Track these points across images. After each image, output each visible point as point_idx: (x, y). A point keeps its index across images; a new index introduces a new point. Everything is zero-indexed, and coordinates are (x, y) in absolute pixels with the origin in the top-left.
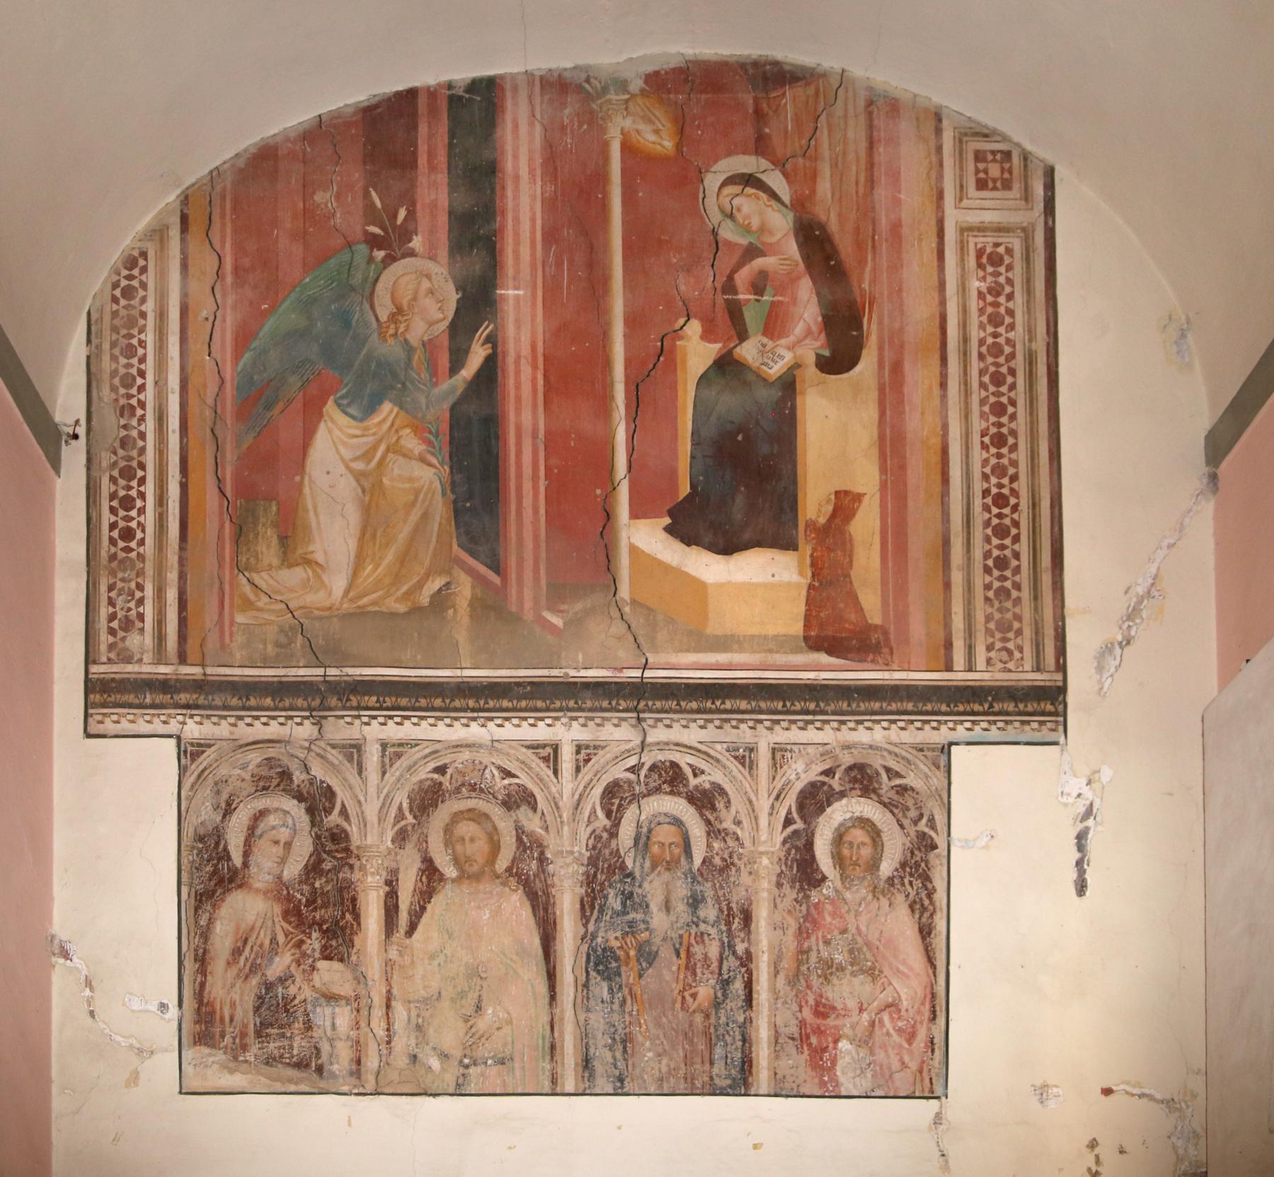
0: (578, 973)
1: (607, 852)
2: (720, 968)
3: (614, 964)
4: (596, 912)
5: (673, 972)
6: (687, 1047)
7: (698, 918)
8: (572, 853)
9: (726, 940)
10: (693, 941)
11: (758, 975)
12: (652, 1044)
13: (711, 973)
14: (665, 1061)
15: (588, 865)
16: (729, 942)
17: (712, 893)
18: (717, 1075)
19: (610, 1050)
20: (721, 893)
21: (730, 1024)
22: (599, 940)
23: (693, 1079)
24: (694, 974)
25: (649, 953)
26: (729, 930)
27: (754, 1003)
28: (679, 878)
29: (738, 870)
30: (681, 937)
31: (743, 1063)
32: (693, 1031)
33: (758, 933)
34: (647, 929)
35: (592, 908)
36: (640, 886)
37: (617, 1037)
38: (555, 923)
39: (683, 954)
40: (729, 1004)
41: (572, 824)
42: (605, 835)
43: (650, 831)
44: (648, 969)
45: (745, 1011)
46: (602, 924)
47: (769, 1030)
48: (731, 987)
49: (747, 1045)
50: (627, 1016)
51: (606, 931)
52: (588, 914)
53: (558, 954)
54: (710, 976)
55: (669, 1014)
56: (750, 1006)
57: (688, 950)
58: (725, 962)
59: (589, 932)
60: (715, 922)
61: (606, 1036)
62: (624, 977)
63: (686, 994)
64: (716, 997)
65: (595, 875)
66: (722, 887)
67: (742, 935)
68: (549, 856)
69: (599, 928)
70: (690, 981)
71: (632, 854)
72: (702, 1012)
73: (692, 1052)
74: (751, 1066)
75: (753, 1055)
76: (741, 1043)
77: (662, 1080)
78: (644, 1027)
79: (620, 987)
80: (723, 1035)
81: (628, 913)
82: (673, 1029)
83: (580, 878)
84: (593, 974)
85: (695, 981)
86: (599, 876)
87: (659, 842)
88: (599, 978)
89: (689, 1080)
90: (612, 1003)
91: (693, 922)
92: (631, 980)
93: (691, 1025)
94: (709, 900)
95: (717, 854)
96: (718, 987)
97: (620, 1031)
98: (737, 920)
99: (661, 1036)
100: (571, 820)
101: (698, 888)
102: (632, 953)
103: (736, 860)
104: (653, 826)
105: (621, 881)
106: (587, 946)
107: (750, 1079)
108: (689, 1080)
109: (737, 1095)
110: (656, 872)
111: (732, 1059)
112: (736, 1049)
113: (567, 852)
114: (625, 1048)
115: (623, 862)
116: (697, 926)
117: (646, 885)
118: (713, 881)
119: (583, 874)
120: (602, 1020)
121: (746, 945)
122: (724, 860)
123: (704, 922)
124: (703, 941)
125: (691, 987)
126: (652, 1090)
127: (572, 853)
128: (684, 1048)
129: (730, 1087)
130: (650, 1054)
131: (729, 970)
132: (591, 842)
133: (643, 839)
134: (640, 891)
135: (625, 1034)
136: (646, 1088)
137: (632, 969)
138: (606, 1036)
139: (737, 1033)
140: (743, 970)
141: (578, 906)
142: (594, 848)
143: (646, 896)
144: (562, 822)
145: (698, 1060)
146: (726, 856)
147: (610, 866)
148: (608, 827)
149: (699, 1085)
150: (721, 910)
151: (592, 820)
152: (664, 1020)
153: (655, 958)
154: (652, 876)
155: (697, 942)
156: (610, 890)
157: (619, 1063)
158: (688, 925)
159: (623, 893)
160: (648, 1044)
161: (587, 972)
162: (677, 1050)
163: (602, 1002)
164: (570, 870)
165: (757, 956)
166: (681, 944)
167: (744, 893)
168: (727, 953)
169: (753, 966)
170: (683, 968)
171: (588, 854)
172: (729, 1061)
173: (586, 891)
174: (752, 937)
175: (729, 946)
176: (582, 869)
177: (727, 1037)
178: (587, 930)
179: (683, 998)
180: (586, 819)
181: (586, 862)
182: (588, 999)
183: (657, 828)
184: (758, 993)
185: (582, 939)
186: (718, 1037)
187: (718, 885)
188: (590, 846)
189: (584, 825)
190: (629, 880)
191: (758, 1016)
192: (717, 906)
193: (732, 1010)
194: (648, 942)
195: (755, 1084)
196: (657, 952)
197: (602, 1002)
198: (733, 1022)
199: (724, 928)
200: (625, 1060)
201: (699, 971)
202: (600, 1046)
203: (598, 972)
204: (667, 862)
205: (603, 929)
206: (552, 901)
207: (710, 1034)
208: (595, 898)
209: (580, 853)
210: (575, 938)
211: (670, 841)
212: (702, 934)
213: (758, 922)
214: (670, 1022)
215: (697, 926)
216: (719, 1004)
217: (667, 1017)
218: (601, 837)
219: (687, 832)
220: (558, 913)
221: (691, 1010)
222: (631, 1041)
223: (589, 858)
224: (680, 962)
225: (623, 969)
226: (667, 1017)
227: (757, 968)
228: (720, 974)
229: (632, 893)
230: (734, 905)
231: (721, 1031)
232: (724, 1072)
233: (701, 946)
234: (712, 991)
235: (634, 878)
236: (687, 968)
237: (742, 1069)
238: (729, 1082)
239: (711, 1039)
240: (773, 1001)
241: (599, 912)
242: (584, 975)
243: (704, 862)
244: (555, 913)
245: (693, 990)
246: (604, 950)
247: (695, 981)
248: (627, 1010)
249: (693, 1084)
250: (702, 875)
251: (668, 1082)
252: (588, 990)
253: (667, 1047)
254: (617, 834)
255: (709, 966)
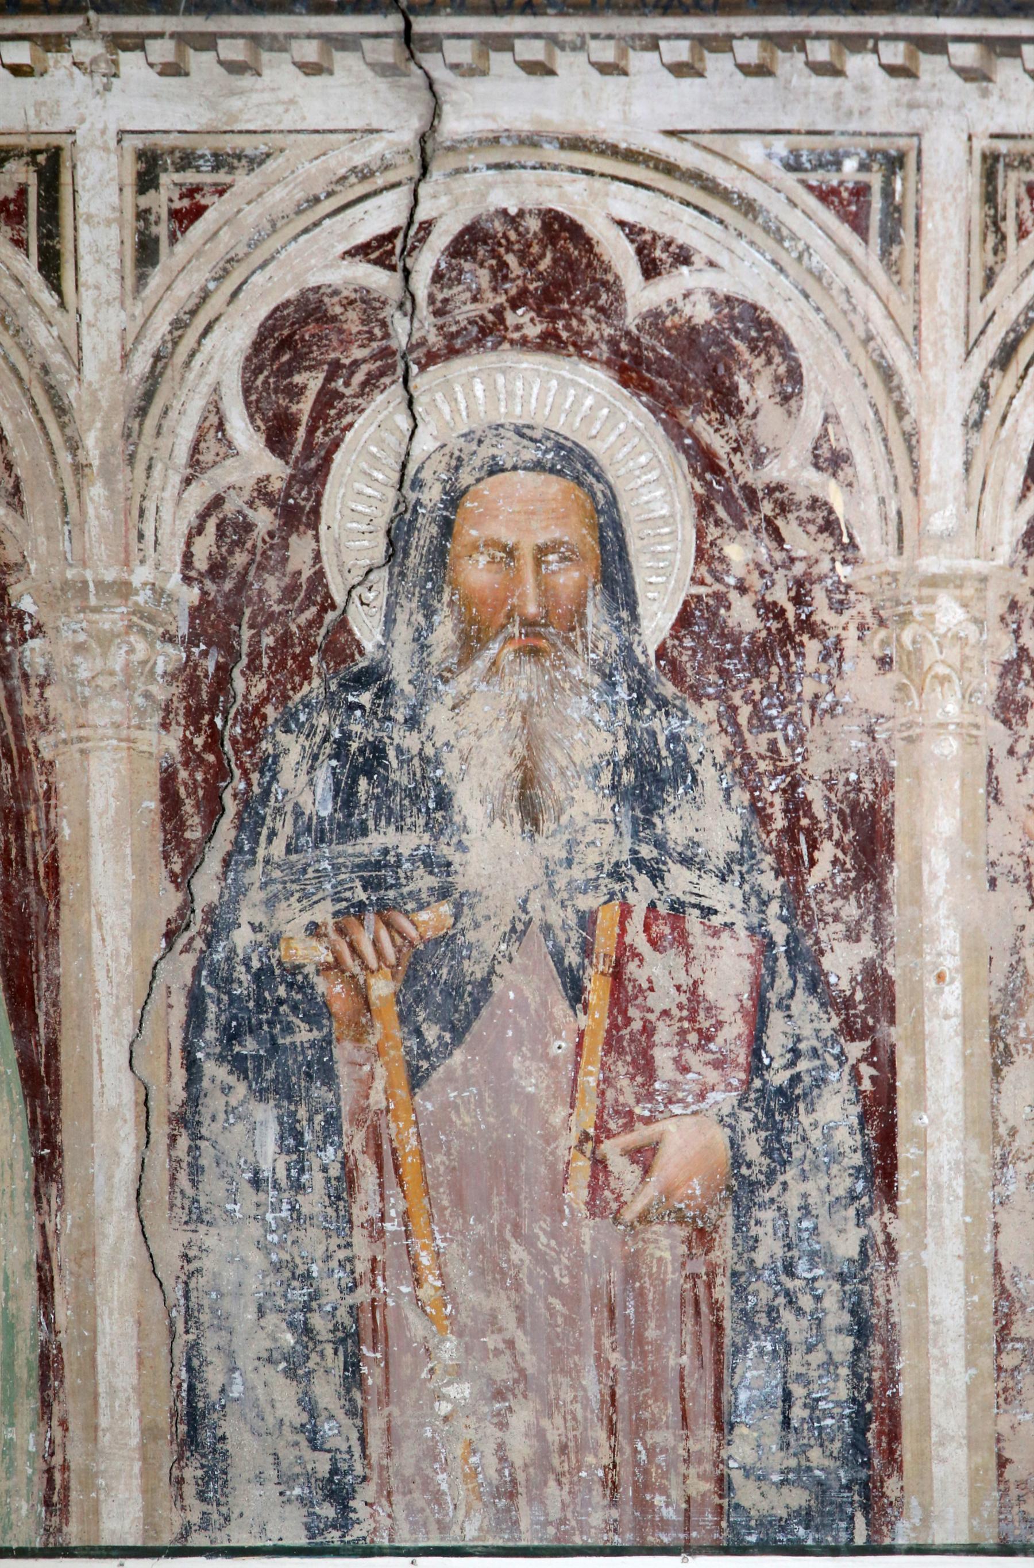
0: (152, 1069)
1: (272, 585)
2: (756, 1044)
3: (304, 1034)
4: (226, 829)
5: (553, 1064)
6: (615, 1358)
7: (660, 844)
8: (124, 589)
9: (779, 932)
10: (635, 936)
11: (920, 1067)
12: (468, 1350)
13: (718, 1064)
14: (522, 1417)
15: (192, 640)
16: (793, 939)
17: (721, 743)
18: (747, 1472)
19: (291, 1373)
20: (757, 743)
21: (802, 1267)
22: (242, 937)
23: (643, 1487)
24: (645, 1067)
25: (453, 990)
26: (795, 893)
27: (904, 1180)
28: (580, 687)
29: (833, 652)
30: (587, 921)
31: (860, 1422)
32: (641, 1294)
33: (917, 900)
34: (444, 893)
35: (213, 810)
36: (413, 722)
37: (319, 1323)
38: (53, 870)
39: (597, 989)
40: (796, 1188)
41: (122, 477)
42: (264, 519)
43: (454, 499)
44: (446, 1050)
45: (862, 1216)
46: (255, 875)
47: (971, 1288)
48: (805, 1119)
49: (876, 1348)
50: (359, 1238)
51: (271, 902)
52: (194, 834)
53: (68, 994)
54: (712, 1076)
55: (540, 1230)
56: (889, 1194)
57: (617, 975)
58: (776, 1018)
59: (199, 906)
60: (732, 859)
61: (272, 1319)
62: (346, 1085)
63: (610, 1148)
64: (738, 1160)
65: (223, 676)
66: (761, 721)
67: (851, 910)
68: (27, 604)
69: (241, 891)
70: (628, 1098)
71: (377, 594)
72: (681, 1220)
73: (640, 1380)
74: (894, 1435)
75: (903, 1388)
76: (848, 1342)
77: (512, 1495)
78: (432, 1281)
79: (332, 1121)
80: (772, 1311)
81: (364, 832)
82: (554, 1288)
83: (161, 692)
84: (214, 1071)
85: (650, 1096)
86: (239, 684)
87: (493, 543)
88: (241, 1089)
89: (627, 1492)
90: (298, 1187)
91: (639, 863)
92: (377, 1098)
93: (631, 1275)
94: (707, 773)
95: (742, 589)
96: (746, 1120)
97: (331, 1297)
98: (827, 851)
99: (508, 1319)
100: (118, 460)
101: (662, 726)
102: (381, 988)
103: (822, 613)
104: (466, 478)
105: (330, 701)
106: (190, 960)
107: (892, 1487)
108: (627, 1492)
109: (834, 1551)
110: (481, 664)
111: (812, 1404)
112: (830, 1364)
113: (100, 584)
114: (353, 1366)
115: (342, 624)
116: (656, 876)
117: (437, 716)
118: (721, 696)
119: (171, 677)
120: (256, 1258)
121: (866, 949)
122: (770, 610)
123: (686, 861)
124: (682, 940)
125: (630, 1119)
126: (471, 1533)
127: (124, 589)
128: (601, 1362)
129: (806, 1518)
130: (461, 1391)
131: (796, 1053)
132: (204, 547)
133: (427, 531)
134: (412, 741)
135: (354, 1311)
136: (443, 1528)
137: (379, 1052)
138: (272, 1319)
139: (830, 1302)
140: (856, 1049)
141: (152, 804)
142: (217, 569)
143: (439, 764)
144: (79, 468)
145: (671, 1411)
146: (780, 595)
147: (285, 640)
148: (276, 485)
149: (669, 1514)
150: (759, 812)
151: (207, 458)
152: (518, 1253)
153: (476, 1007)
154: (462, 682)
155: (653, 943)
156: (282, 737)
157: (327, 1428)
158: (616, 874)
159: (340, 750)
160: (449, 1349)
161: (191, 1065)
162: (574, 1374)
163: (256, 1182)
164: (118, 660)
165: (917, 991)
166: (587, 950)
167: (858, 743)
168: (783, 983)
169: (896, 1034)
170: (595, 1046)
171: (192, 595)
172: (798, 1413)
173: (187, 744)
174: (894, 918)
175: (792, 957)
176: (175, 654)
177: (787, 1317)
178: (188, 906)
179: (599, 1164)
180: (182, 454)
181: (184, 630)
182: (196, 1170)
183: (485, 488)
184: (920, 1137)
185: (170, 936)
186: (747, 1317)
187: (745, 712)
188: (201, 563)
189: (175, 479)
190: (365, 698)
191: (920, 1233)
192: (741, 796)
193: (806, 1209)
194: (447, 940)
195: (913, 1502)
196: (486, 982)
197: (256, 1182)
198: (813, 1256)
199: (771, 883)
200: (355, 1412)
201: (663, 1057)
202: (246, 1360)
203: (238, 1065)
204: (529, 623)
205: (256, 895)
206: (40, 786)
207: (716, 1307)
208: (222, 772)
209: (158, 592)
210: (139, 927)
211: (542, 539)
212: (678, 908)
213: (918, 856)
214: (540, 1258)
215: (656, 876)
216: (752, 1186)
217: (529, 1242)
218: (248, 527)
219: (613, 502)
220: (66, 832)
221: (629, 1215)
222: (379, 1336)
223: (195, 613)
224: (583, 1021)
225: (343, 1052)
226: (529, 1242)
227: (918, 1038)
228: (756, 1067)
229: (377, 750)
230: (813, 792)
231: (762, 1293)
232: (777, 1460)
233: (674, 958)
234: (722, 1136)
235: (386, 691)
236: (612, 1043)
237: (858, 1446)
238: (798, 1498)
239: (718, 1326)
240: (984, 1172)
241: (240, 827)
242: (180, 1076)
243: (684, 620)
244: (52, 835)
245: (641, 1134)
246: (263, 976)
247: (650, 1096)
248: (359, 1216)
249: (643, 1506)
250: (676, 673)
251: (538, 1499)
252: (196, 1138)
253: (530, 1363)
254: (316, 511)
255: (707, 1038)
